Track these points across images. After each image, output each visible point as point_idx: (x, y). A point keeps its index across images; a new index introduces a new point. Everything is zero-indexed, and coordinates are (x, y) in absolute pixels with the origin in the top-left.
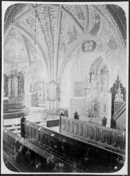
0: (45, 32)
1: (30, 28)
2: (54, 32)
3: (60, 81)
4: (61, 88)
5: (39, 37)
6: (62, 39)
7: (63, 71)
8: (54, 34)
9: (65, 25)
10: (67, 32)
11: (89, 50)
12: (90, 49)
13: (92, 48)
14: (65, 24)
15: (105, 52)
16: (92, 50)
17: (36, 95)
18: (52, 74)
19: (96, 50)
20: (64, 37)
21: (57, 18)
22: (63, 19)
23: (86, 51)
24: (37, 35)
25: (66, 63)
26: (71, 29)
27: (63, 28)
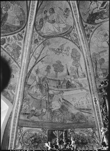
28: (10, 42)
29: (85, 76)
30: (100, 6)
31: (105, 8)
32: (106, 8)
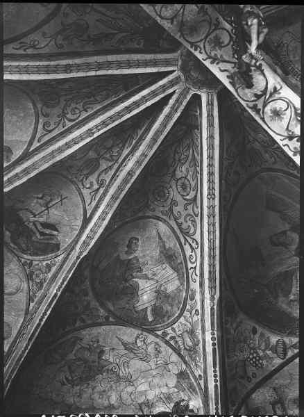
28: (78, 106)
30: (41, 220)
31: (42, 234)
32: (42, 237)
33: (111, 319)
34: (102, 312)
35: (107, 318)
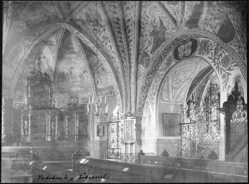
0: (116, 34)
1: (92, 30)
2: (130, 34)
3: (140, 113)
4: (142, 125)
5: (106, 44)
6: (143, 45)
7: (144, 97)
8: (131, 38)
9: (147, 20)
10: (150, 32)
11: (186, 55)
12: (186, 54)
13: (190, 51)
14: (146, 18)
15: (213, 51)
16: (191, 54)
17: (107, 142)
18: (129, 105)
19: (197, 53)
20: (145, 41)
21: (134, 7)
22: (143, 9)
23: (180, 58)
24: (104, 41)
25: (149, 84)
26: (156, 26)
27: (144, 27)
29: (17, 63)
33: (71, 53)
34: (69, 52)
35: (70, 53)
